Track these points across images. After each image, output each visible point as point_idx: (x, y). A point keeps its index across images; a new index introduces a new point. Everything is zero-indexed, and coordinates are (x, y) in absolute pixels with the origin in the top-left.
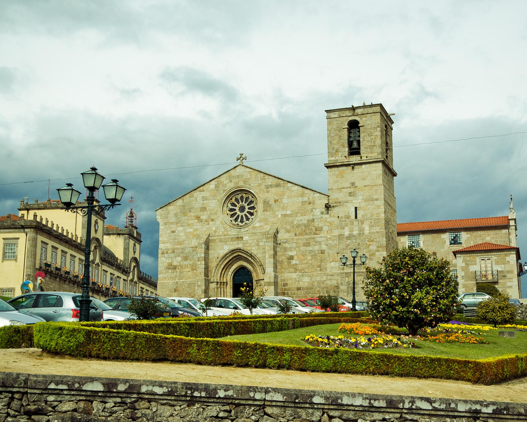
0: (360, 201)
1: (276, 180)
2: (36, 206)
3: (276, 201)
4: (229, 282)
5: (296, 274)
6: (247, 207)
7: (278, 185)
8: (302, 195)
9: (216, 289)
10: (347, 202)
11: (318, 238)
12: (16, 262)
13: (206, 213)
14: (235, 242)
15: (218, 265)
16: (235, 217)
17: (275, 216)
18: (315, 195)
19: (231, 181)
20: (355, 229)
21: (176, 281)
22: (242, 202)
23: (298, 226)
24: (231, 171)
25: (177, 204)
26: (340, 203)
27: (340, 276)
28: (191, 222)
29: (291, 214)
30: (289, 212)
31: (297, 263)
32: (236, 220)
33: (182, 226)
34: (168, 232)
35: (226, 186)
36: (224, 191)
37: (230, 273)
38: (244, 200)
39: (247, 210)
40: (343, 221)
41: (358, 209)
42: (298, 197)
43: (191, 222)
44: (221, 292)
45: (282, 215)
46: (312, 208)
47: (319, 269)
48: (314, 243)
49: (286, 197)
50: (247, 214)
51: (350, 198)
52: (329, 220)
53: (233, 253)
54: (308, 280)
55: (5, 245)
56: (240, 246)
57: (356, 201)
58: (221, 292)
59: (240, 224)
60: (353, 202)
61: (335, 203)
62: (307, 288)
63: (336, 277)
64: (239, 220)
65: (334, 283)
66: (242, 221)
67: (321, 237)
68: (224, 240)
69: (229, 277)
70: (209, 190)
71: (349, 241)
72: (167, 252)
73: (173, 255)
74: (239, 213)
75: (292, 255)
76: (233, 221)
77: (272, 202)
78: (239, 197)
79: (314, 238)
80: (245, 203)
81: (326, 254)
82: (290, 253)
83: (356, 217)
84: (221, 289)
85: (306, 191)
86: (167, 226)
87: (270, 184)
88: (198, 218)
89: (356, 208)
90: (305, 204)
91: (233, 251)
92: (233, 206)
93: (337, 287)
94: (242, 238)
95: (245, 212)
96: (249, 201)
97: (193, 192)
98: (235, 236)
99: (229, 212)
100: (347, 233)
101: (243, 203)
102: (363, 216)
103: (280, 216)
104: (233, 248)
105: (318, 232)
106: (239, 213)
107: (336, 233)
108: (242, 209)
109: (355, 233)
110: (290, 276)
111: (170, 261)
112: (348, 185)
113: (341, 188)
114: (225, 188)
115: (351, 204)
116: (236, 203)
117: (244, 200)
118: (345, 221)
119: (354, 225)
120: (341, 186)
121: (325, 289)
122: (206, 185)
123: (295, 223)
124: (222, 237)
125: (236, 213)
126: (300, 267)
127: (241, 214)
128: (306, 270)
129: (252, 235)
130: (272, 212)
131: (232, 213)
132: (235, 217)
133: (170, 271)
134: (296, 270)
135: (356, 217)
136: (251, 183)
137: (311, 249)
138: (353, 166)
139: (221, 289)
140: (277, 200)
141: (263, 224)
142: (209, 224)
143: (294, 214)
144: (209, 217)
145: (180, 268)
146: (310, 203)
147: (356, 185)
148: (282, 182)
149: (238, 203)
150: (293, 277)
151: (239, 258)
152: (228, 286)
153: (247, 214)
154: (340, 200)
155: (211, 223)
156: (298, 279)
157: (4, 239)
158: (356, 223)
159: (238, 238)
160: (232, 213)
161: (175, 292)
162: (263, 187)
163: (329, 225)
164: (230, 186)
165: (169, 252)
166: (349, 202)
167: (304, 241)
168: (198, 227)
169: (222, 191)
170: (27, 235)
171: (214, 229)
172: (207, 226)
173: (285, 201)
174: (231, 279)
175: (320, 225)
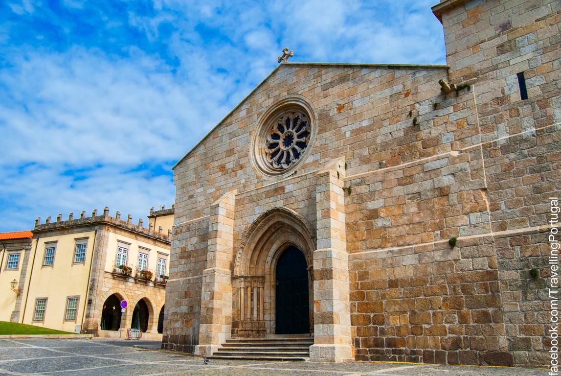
0: (530, 56)
1: (339, 72)
2: (162, 213)
3: (340, 108)
4: (267, 277)
5: (386, 250)
6: (295, 135)
7: (343, 80)
8: (391, 83)
9: (242, 291)
10: (495, 68)
11: (430, 162)
12: (84, 265)
13: (233, 158)
14: (272, 199)
16: (278, 156)
17: (340, 136)
18: (417, 75)
19: (269, 96)
20: (525, 124)
21: (189, 278)
22: (288, 128)
23: (385, 146)
24: (270, 81)
25: (198, 153)
26: (476, 75)
27: (494, 245)
29: (370, 125)
30: (365, 124)
31: (388, 224)
32: (279, 162)
33: (202, 186)
34: (184, 199)
35: (261, 107)
36: (259, 115)
37: (269, 259)
38: (291, 123)
39: (296, 140)
40: (488, 113)
41: (526, 76)
42: (381, 89)
43: (213, 176)
44: (252, 295)
45: (352, 132)
46: (412, 103)
47: (439, 232)
48: (421, 175)
49: (359, 96)
50: (297, 147)
51: (504, 58)
52: (453, 118)
54: (413, 262)
55: (78, 246)
56: (280, 204)
57: (519, 59)
58: (252, 295)
59: (285, 166)
60: (512, 62)
61: (465, 77)
62: (412, 283)
63: (484, 249)
64: (283, 160)
65: (482, 263)
66: (288, 162)
67: (438, 159)
68: (255, 198)
69: (267, 266)
70: (238, 120)
71: (512, 156)
72: (181, 231)
73: (187, 234)
74: (283, 148)
75: (375, 207)
76: (274, 165)
77: (334, 112)
79: (421, 164)
80: (293, 129)
81: (454, 198)
82: (371, 205)
84: (252, 290)
85: (398, 73)
86: (185, 190)
87: (329, 81)
88: (222, 168)
89: (521, 77)
90: (398, 99)
91: (266, 214)
93: (491, 275)
94: (283, 188)
95: (294, 145)
96: (299, 122)
97: (217, 130)
98: (273, 187)
99: (267, 151)
100: (503, 137)
101: (290, 130)
102: (543, 87)
103: (348, 135)
104: (264, 209)
105: (430, 150)
106: (283, 148)
107: (477, 142)
108: (288, 140)
109: (529, 130)
110: (374, 256)
111: (184, 245)
112: (491, 32)
113: (477, 44)
114: (260, 110)
115: (507, 69)
116: (279, 133)
117: (291, 123)
118: (496, 111)
120: (474, 40)
121: (458, 283)
122: (235, 115)
123: (379, 141)
124: (253, 193)
125: (279, 150)
126: (393, 232)
127: (287, 148)
128: (408, 239)
129: (299, 179)
130: (334, 131)
131: (273, 150)
132: (278, 156)
133: (183, 261)
134: (385, 241)
136: (299, 89)
137: (416, 189)
139: (252, 290)
140: (343, 106)
141: (318, 157)
142: (236, 175)
143: (378, 122)
144: (238, 162)
145: (195, 255)
146: (407, 95)
147: (514, 26)
148: (350, 72)
149: (282, 131)
150: (380, 256)
151: (278, 228)
152: (267, 284)
153: (297, 147)
154: (477, 67)
155: (240, 172)
156: (389, 261)
157: (76, 239)
158: (525, 110)
159: (276, 190)
160: (273, 150)
161: (186, 298)
162: (318, 90)
163: (454, 128)
164: (265, 102)
165: (184, 230)
166: (500, 66)
167: (400, 174)
168: (222, 183)
169: (256, 116)
170: (96, 233)
171: (243, 181)
172: (235, 179)
173: (357, 104)
174: (272, 270)
175: (434, 133)
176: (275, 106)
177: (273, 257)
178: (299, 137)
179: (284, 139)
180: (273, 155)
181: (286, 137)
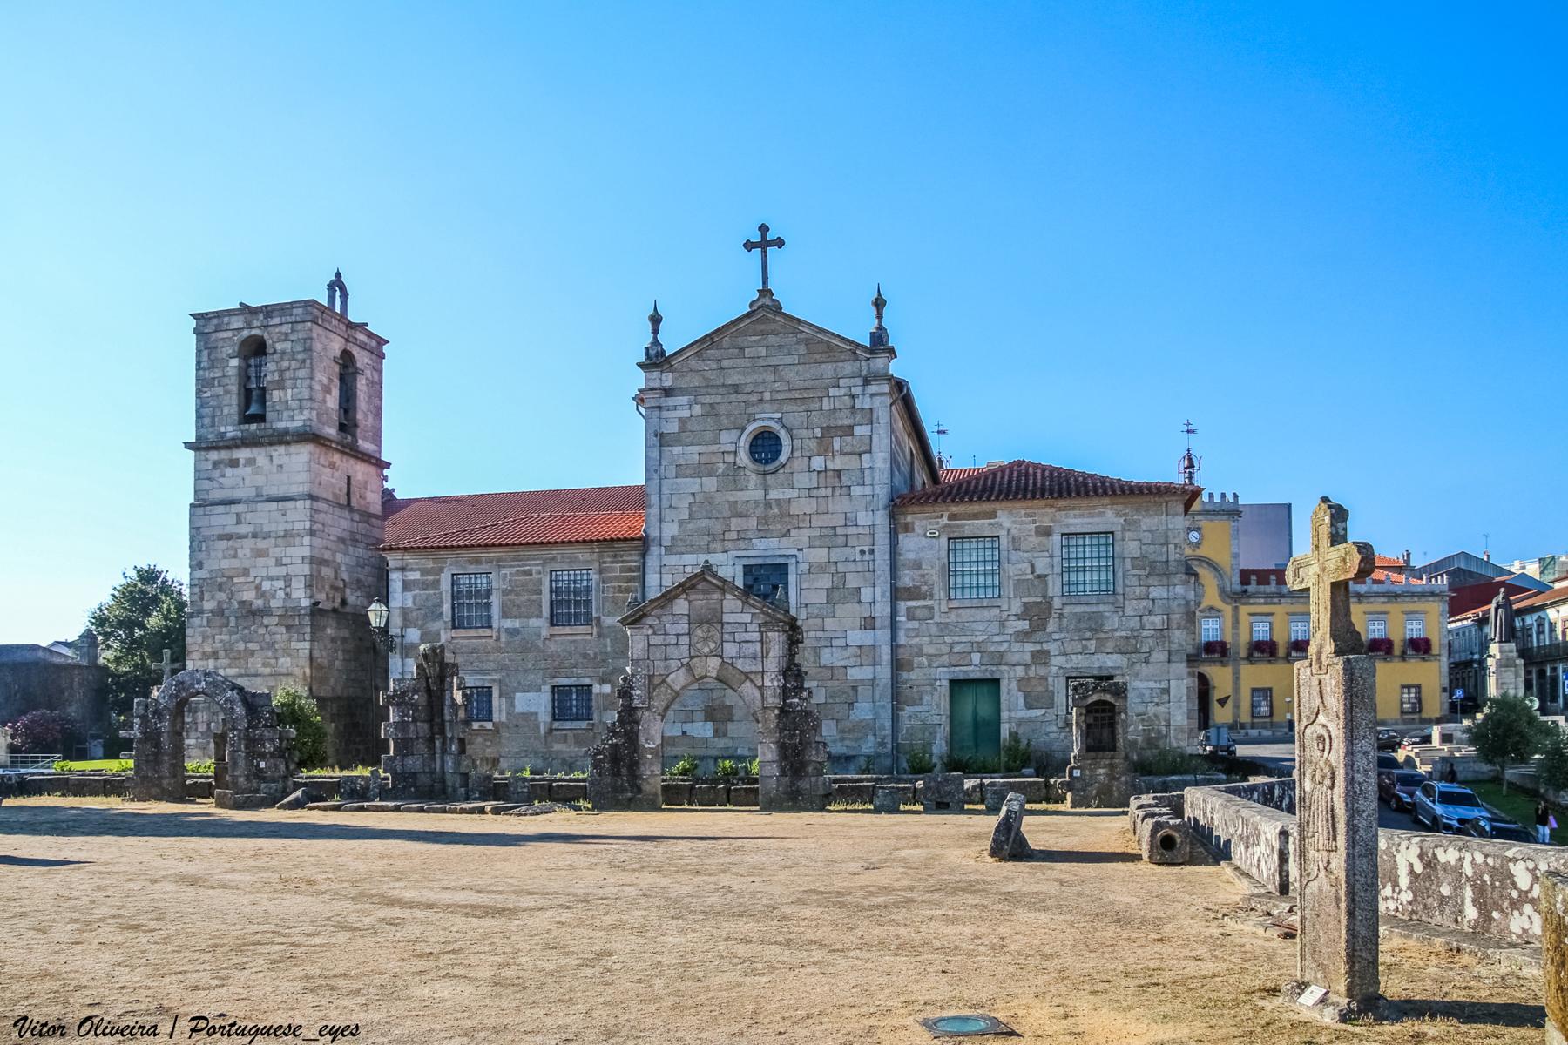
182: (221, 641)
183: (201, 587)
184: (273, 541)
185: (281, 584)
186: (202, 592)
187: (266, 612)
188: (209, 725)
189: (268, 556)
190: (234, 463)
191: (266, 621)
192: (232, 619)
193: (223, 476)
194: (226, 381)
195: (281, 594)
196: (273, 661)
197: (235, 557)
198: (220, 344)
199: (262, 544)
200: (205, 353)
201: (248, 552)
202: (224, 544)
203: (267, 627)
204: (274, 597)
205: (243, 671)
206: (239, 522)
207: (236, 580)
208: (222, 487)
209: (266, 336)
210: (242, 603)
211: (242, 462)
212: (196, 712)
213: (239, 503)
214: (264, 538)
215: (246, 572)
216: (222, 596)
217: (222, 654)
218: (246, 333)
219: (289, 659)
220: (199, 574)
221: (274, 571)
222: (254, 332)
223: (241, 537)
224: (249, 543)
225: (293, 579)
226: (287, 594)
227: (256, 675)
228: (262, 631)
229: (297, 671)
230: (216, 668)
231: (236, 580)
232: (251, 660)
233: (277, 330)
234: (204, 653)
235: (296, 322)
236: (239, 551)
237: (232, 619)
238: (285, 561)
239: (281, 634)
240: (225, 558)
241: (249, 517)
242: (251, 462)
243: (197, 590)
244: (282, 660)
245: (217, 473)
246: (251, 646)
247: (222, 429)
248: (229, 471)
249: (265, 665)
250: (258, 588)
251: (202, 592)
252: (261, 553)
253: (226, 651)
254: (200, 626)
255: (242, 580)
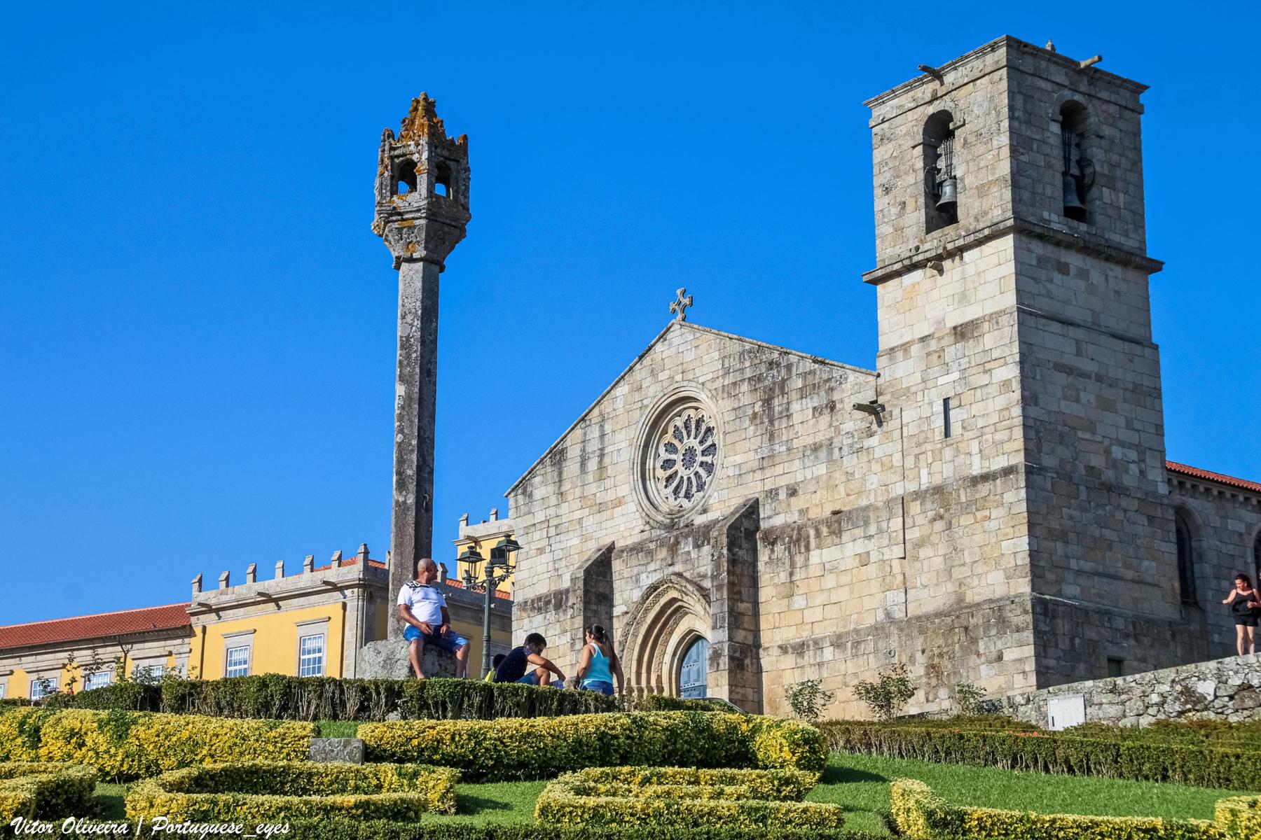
15: (627, 635)
28: (577, 515)
37: (667, 658)
39: (700, 458)
41: (952, 403)
53: (659, 596)
66: (688, 496)
74: (683, 472)
78: (679, 422)
80: (695, 438)
83: (947, 433)
89: (946, 401)
92: (670, 453)
119: (943, 461)
127: (688, 472)
132: (674, 484)
135: (947, 433)
138: (937, 262)
158: (948, 454)
160: (669, 472)
176: (666, 397)
177: (674, 655)
178: (703, 453)
179: (684, 455)
180: (669, 479)
181: (686, 450)
182: (1071, 518)
183: (1037, 432)
184: (1121, 392)
185: (1133, 455)
186: (1039, 439)
187: (1123, 491)
188: (1072, 640)
189: (1116, 412)
190: (1063, 269)
191: (1124, 502)
192: (1082, 488)
193: (1051, 281)
194: (1047, 150)
195: (1134, 468)
196: (1135, 562)
197: (1077, 400)
198: (1037, 95)
199: (1108, 393)
200: (1019, 99)
201: (1092, 397)
202: (1062, 378)
203: (1125, 511)
204: (1126, 471)
205: (1101, 569)
206: (1079, 353)
207: (1080, 434)
208: (1050, 296)
209: (1090, 109)
210: (1090, 469)
211: (1073, 270)
212: (1054, 617)
213: (1079, 326)
214: (1110, 386)
215: (1091, 426)
216: (1066, 453)
217: (1072, 536)
218: (1067, 94)
219: (1153, 564)
220: (1033, 412)
221: (1126, 435)
222: (1077, 97)
223: (1086, 375)
224: (1091, 385)
225: (1148, 452)
226: (1141, 472)
227: (1115, 577)
228: (1119, 515)
229: (1167, 586)
230: (1067, 557)
231: (1080, 434)
232: (1109, 554)
233: (1104, 107)
234: (1050, 530)
235: (1126, 108)
236: (1082, 394)
237: (1082, 488)
238: (1137, 425)
239: (1142, 527)
240: (1065, 398)
241: (1091, 349)
242: (1083, 274)
243: (1032, 434)
244: (1146, 563)
245: (1043, 274)
246: (1108, 533)
247: (1046, 215)
248: (1057, 277)
249: (1127, 566)
250: (1107, 452)
251: (1039, 439)
252: (1108, 406)
253: (1078, 534)
254: (1043, 489)
255: (1087, 436)
